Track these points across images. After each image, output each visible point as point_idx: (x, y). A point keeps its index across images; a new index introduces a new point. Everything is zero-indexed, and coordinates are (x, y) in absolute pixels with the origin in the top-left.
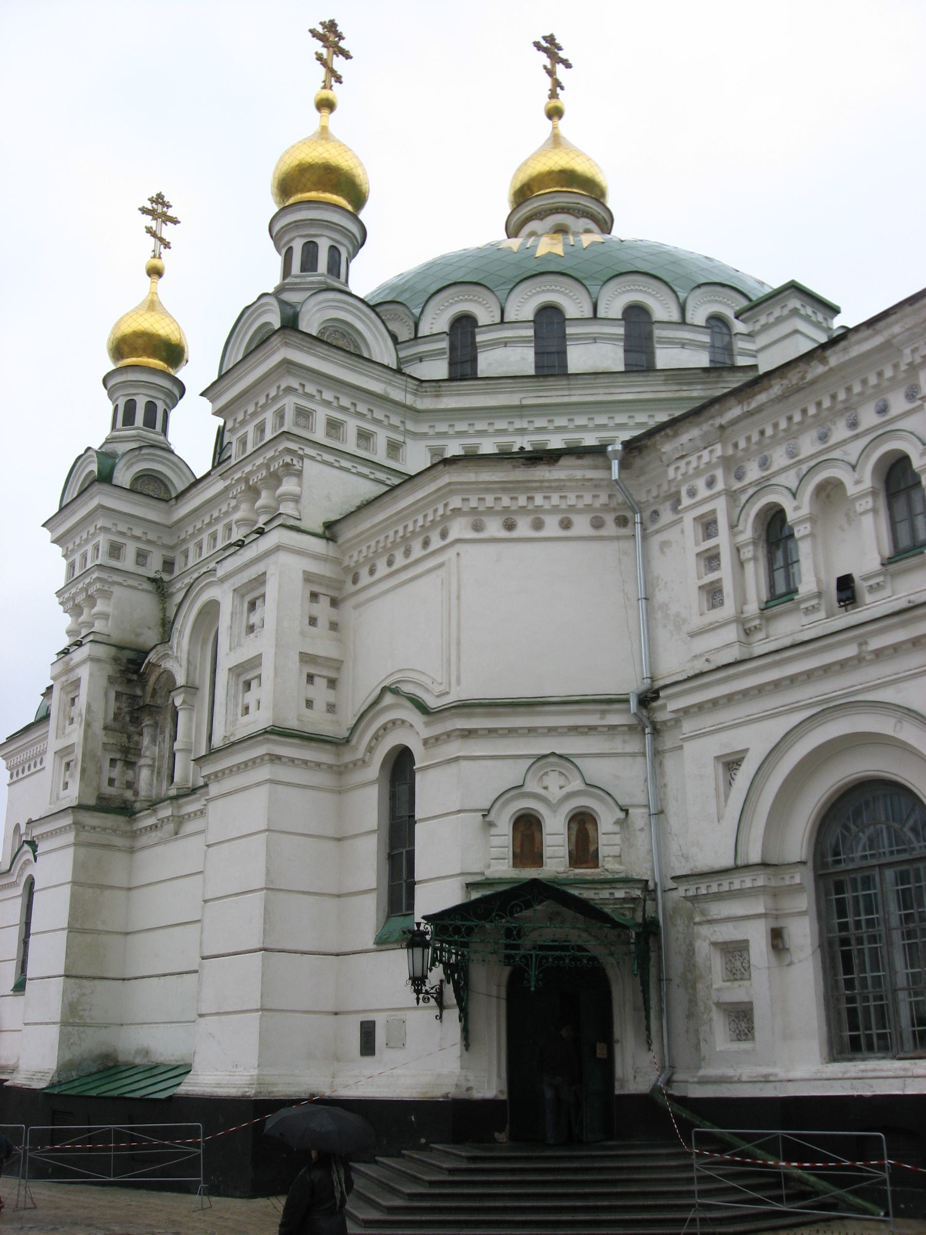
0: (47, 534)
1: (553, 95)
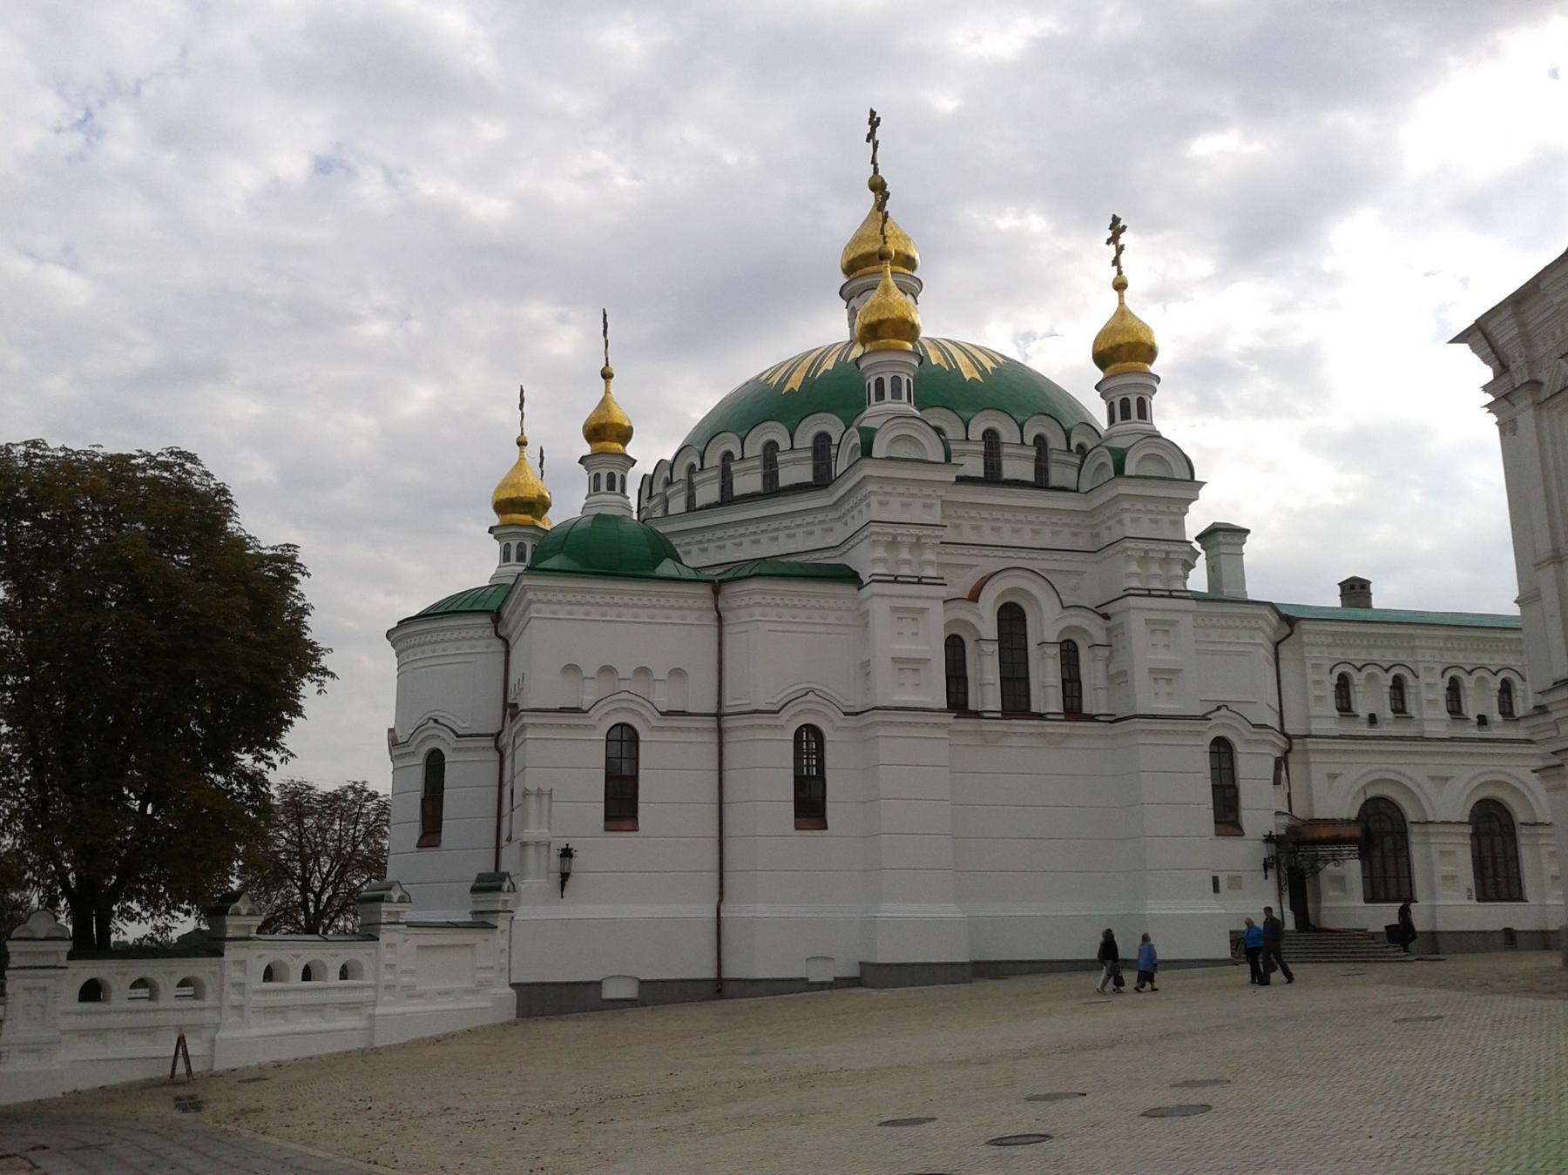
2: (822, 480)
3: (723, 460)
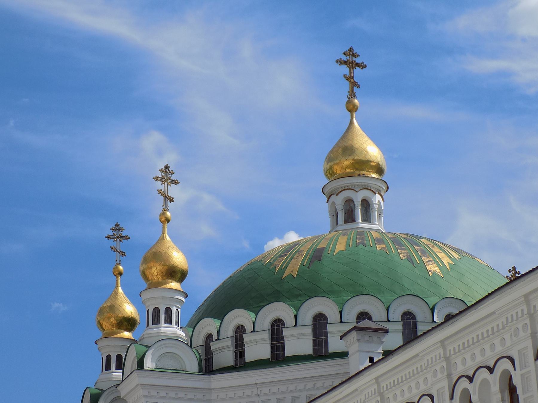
1: (352, 95)
3: (236, 332)
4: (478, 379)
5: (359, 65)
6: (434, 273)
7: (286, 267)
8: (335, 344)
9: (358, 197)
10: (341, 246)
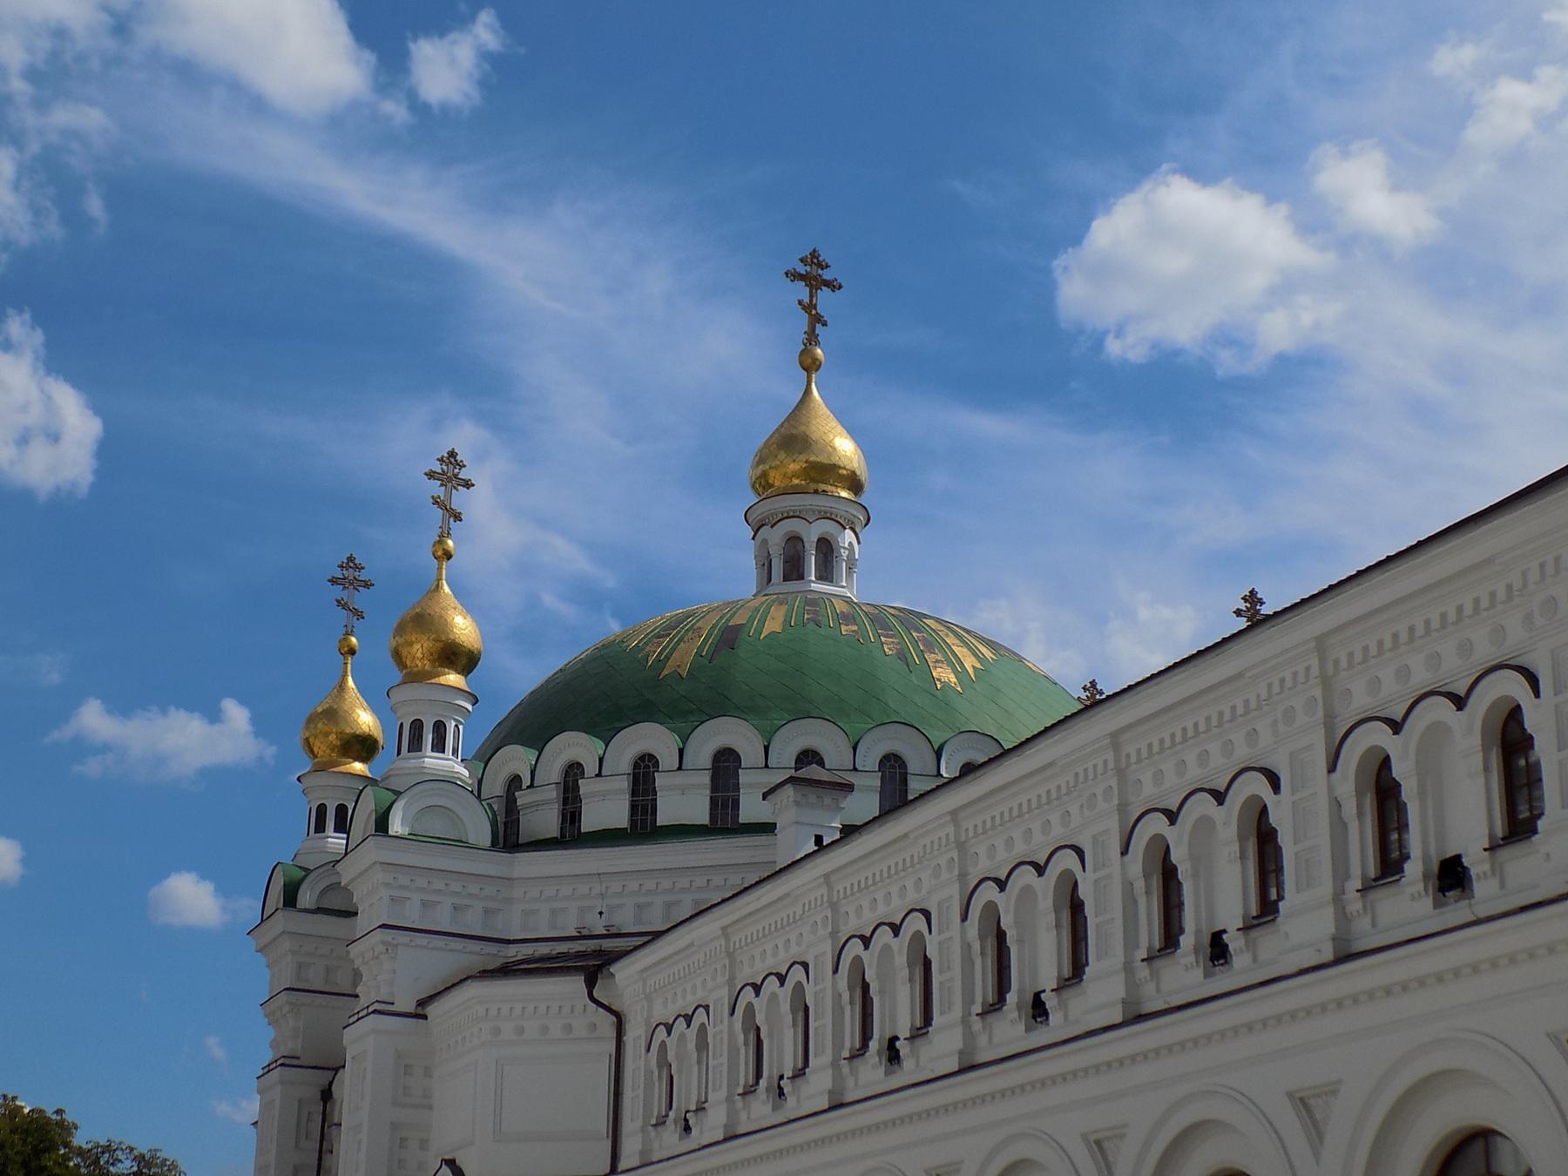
0: (251, 943)
1: (812, 338)
2: (724, 821)
3: (567, 774)
4: (1015, 885)
5: (827, 284)
6: (946, 685)
7: (668, 658)
8: (751, 808)
9: (812, 533)
10: (773, 625)
